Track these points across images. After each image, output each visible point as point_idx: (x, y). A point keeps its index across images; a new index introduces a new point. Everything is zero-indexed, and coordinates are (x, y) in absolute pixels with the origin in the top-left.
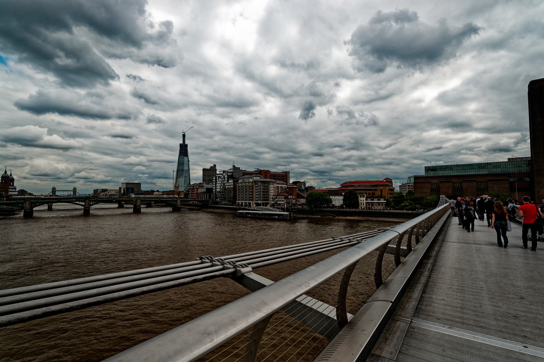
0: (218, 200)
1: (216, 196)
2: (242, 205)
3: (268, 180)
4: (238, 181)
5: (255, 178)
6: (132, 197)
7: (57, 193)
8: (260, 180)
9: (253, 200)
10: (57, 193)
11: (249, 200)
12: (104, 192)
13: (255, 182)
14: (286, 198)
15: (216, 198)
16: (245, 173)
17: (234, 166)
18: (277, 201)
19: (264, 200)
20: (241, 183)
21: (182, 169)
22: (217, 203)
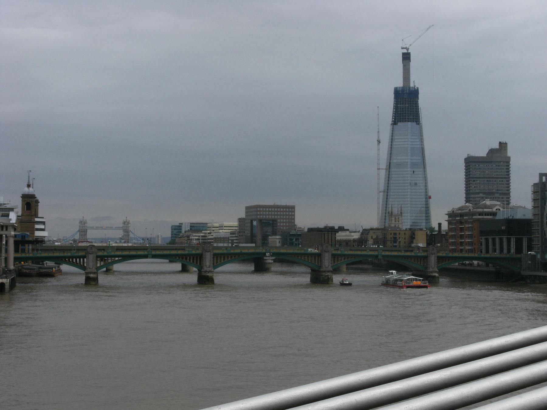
7: (91, 235)
10: (91, 235)
12: (199, 231)
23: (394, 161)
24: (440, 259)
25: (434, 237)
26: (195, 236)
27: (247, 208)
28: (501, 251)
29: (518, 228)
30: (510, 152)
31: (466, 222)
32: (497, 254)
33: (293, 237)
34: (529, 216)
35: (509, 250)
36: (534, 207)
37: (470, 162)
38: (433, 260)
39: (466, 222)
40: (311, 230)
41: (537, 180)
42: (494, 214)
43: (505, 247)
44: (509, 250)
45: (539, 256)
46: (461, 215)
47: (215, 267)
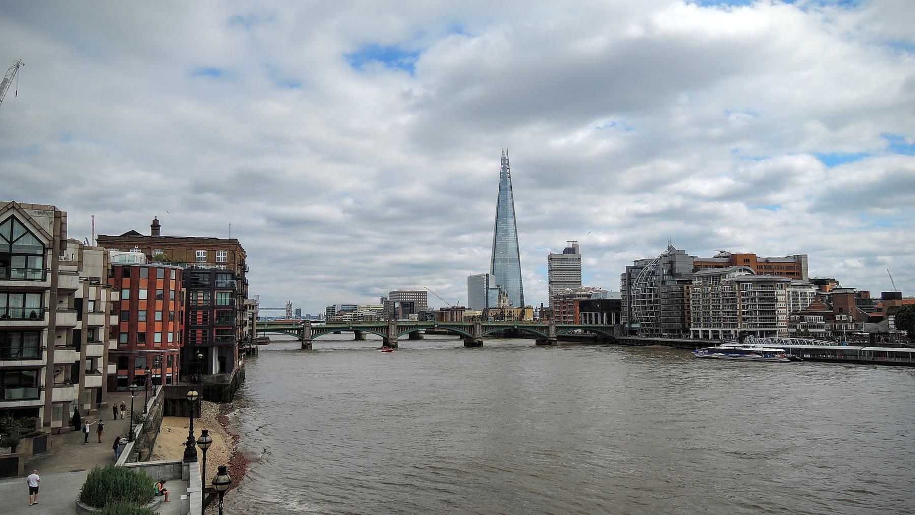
0: (634, 326)
1: (631, 316)
2: (706, 335)
3: (769, 277)
4: (690, 282)
5: (737, 274)
6: (403, 321)
8: (751, 278)
9: (734, 326)
11: (725, 325)
13: (738, 282)
14: (827, 319)
15: (632, 321)
16: (699, 265)
17: (670, 248)
18: (803, 326)
19: (765, 325)
20: (696, 286)
21: (504, 254)
22: (633, 332)
23: (497, 257)
24: (558, 328)
25: (544, 312)
26: (348, 315)
27: (391, 293)
28: (597, 322)
29: (610, 306)
30: (580, 251)
31: (568, 302)
32: (594, 325)
33: (426, 315)
34: (620, 298)
35: (602, 322)
36: (622, 291)
37: (550, 259)
38: (552, 329)
39: (568, 302)
40: (442, 309)
41: (624, 271)
42: (590, 296)
43: (599, 320)
44: (602, 322)
45: (627, 326)
46: (564, 297)
47: (398, 336)
